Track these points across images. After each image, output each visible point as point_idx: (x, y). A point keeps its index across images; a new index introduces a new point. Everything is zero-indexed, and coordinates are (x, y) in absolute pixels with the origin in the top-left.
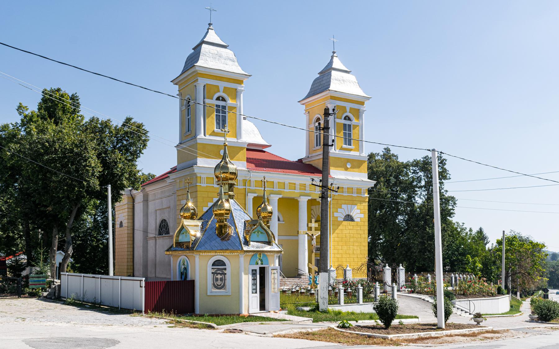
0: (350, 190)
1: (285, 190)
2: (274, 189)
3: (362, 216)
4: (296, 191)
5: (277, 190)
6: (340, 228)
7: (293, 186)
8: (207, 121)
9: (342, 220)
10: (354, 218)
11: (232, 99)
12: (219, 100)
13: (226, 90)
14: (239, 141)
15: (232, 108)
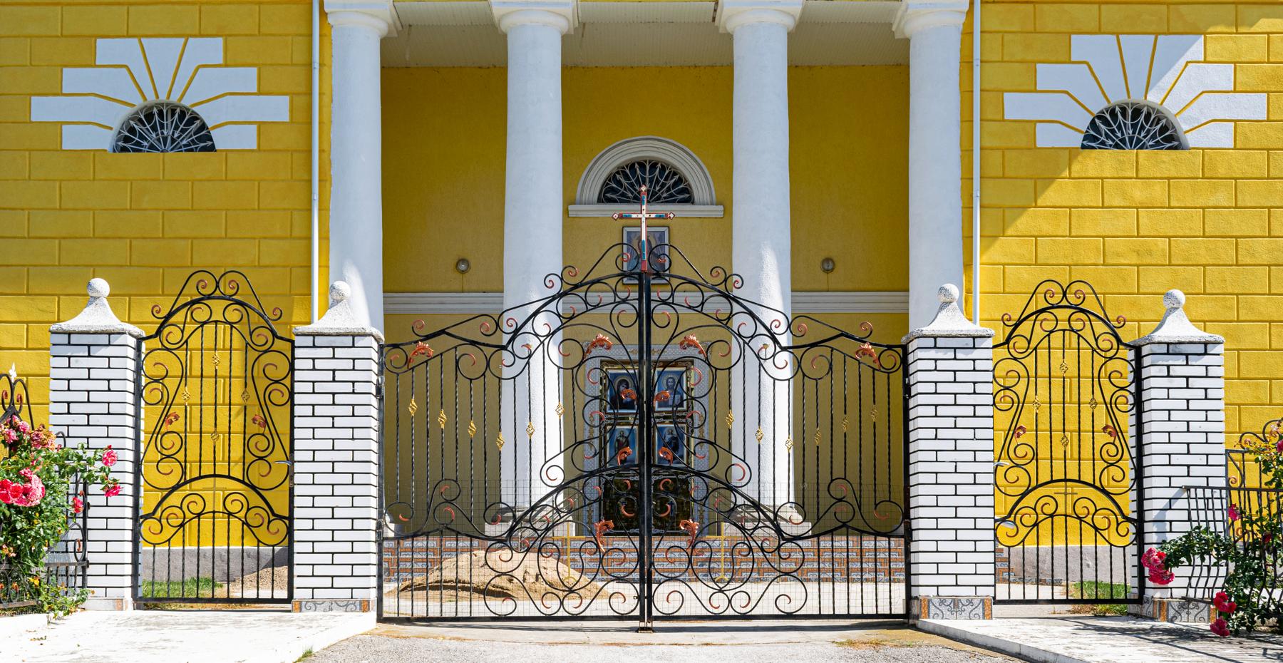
6: (1050, 196)
9: (1078, 140)
10: (1182, 124)
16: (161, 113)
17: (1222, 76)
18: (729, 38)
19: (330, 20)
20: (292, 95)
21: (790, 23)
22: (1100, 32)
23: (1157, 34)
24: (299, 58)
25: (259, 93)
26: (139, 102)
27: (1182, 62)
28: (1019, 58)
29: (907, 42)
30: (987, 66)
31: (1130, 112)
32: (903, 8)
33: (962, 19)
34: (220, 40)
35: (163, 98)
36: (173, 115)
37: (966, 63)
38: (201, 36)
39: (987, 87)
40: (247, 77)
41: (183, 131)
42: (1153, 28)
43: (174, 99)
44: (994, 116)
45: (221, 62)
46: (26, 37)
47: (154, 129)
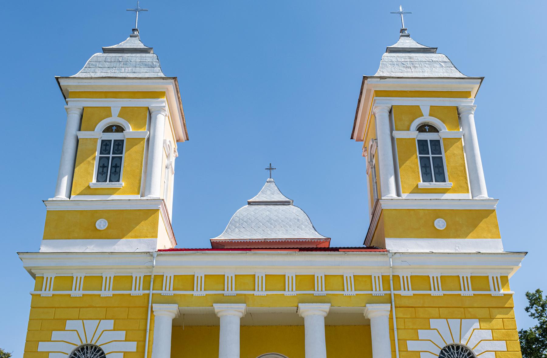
0: (450, 281)
1: (256, 293)
2: (226, 293)
3: (501, 346)
4: (286, 293)
5: (234, 292)
7: (276, 281)
8: (76, 170)
11: (138, 125)
12: (112, 131)
13: (125, 112)
14: (142, 198)
15: (135, 141)
16: (87, 348)
17: (487, 334)
18: (303, 319)
19: (155, 313)
20: (138, 341)
21: (325, 314)
22: (440, 318)
23: (461, 319)
24: (142, 327)
25: (126, 341)
26: (79, 344)
27: (472, 329)
28: (411, 327)
29: (369, 320)
30: (399, 331)
31: (455, 347)
32: (366, 309)
33: (389, 313)
34: (113, 321)
35: (89, 342)
36: (91, 349)
37: (392, 329)
38: (106, 319)
39: (400, 338)
40: (122, 335)
41: (95, 355)
42: (459, 317)
43: (93, 343)
44: (404, 349)
45: (112, 329)
46: (40, 319)
47: (84, 354)
